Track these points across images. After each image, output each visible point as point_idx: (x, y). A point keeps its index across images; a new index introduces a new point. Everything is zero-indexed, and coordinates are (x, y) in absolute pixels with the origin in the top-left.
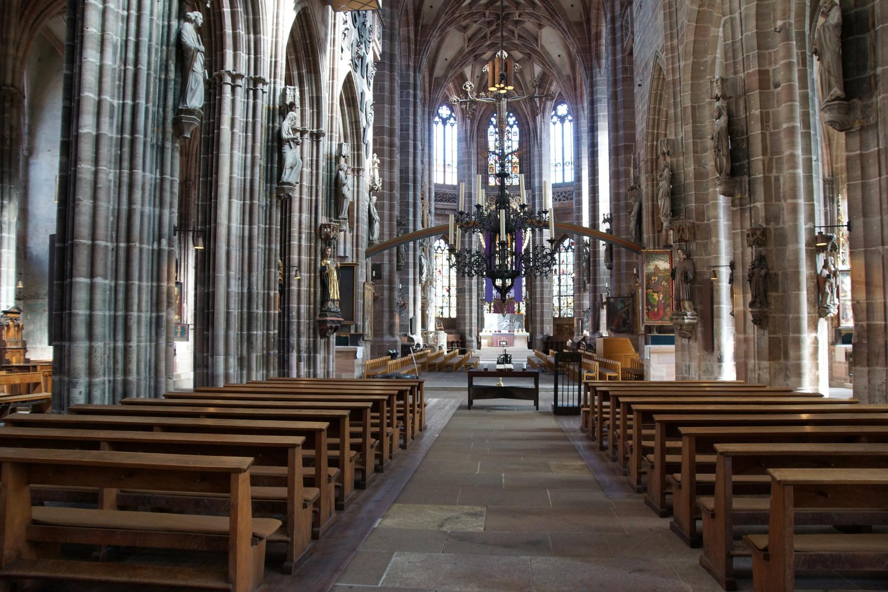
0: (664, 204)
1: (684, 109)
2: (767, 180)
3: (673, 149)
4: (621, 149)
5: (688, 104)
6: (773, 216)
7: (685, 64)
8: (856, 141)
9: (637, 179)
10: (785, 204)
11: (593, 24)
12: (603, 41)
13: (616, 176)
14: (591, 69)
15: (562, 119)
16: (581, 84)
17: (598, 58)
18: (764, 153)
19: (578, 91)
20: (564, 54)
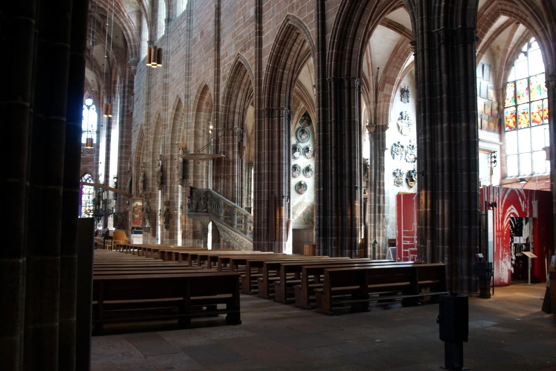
0: (141, 185)
1: (150, 152)
2: (171, 187)
3: (145, 165)
4: (124, 146)
5: (151, 151)
6: (172, 198)
7: (151, 137)
8: (184, 189)
9: (131, 168)
10: (176, 194)
11: (113, 75)
12: (117, 85)
13: (120, 158)
14: (110, 97)
15: (89, 107)
16: (103, 98)
17: (114, 93)
18: (170, 179)
19: (101, 101)
20: (95, 80)
